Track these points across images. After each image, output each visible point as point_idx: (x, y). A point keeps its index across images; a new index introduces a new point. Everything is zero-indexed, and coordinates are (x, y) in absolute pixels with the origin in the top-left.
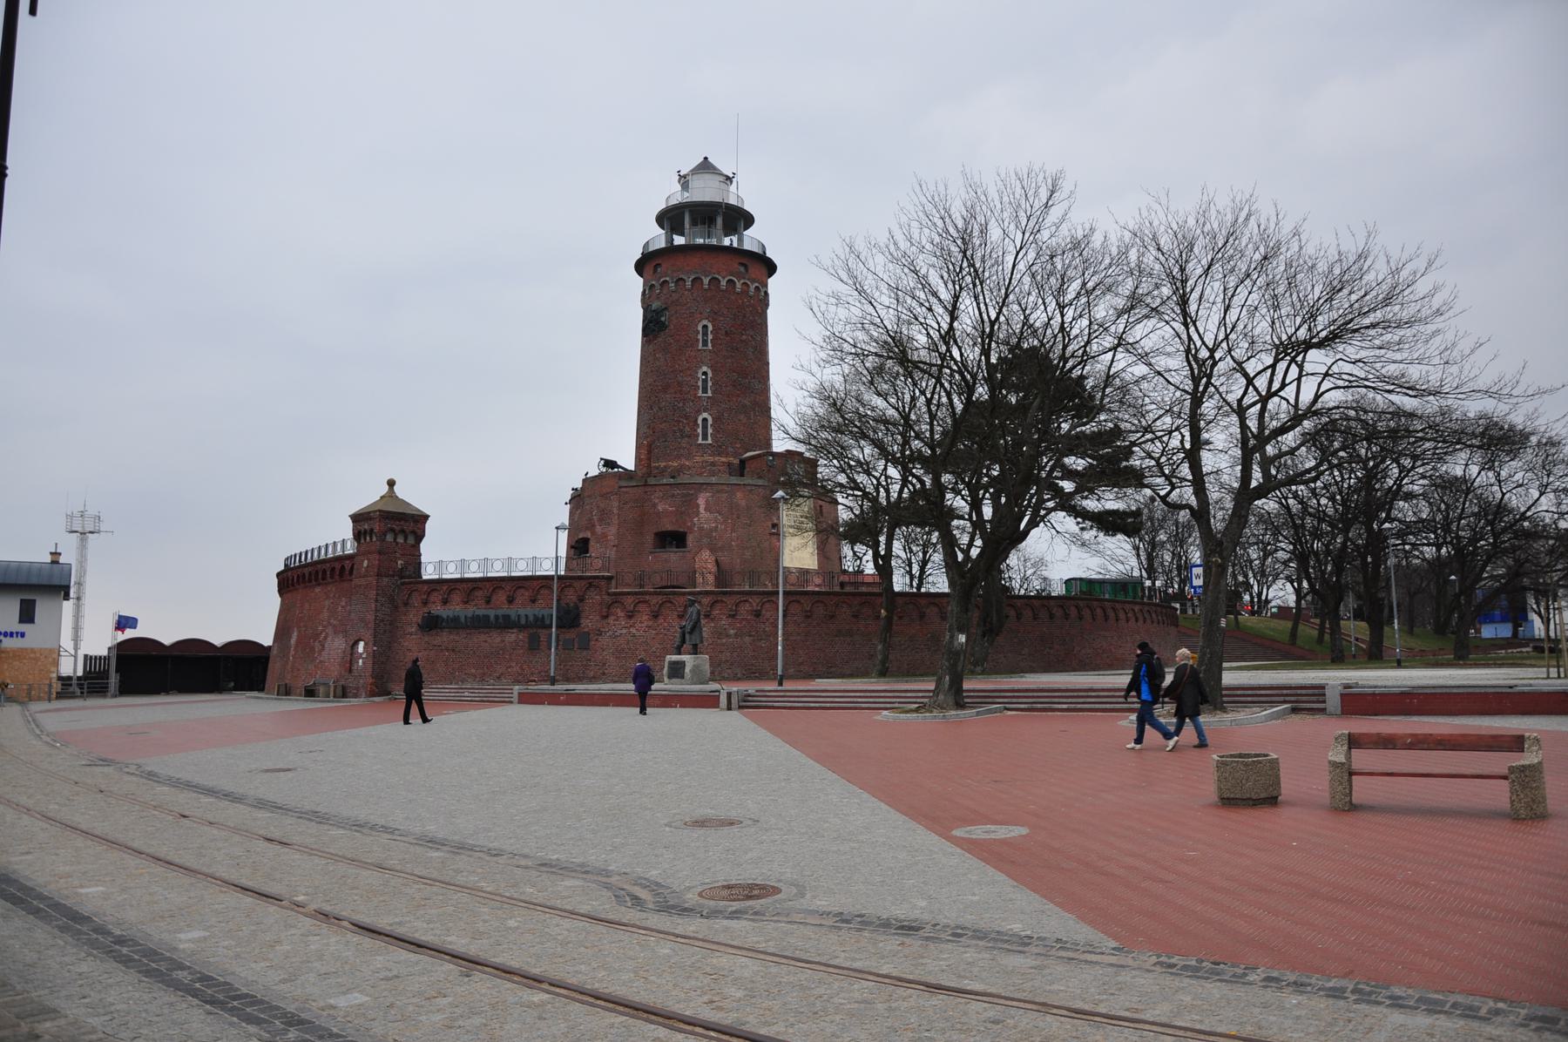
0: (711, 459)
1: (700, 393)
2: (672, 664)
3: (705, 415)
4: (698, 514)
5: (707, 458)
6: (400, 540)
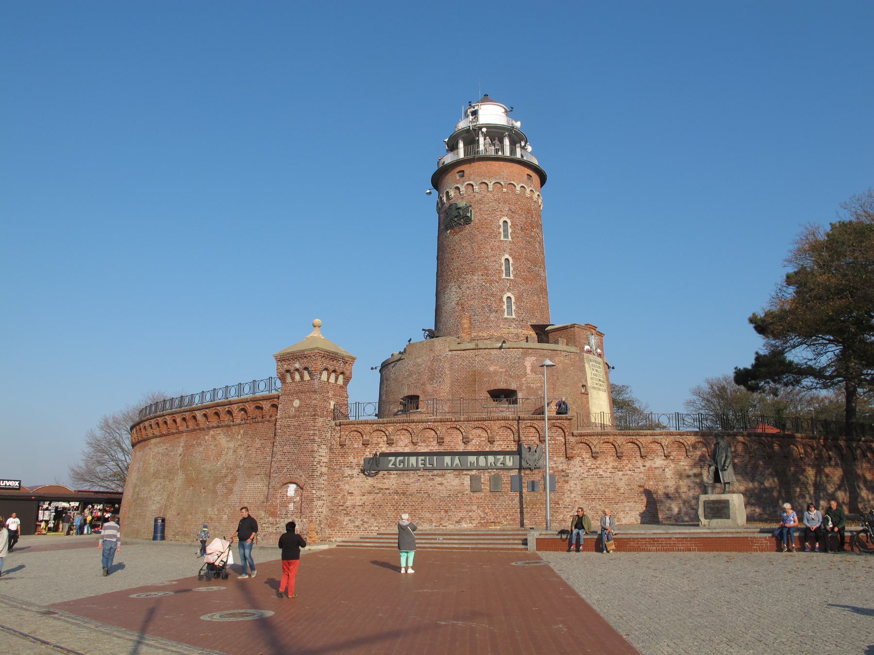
0: (515, 331)
1: (504, 276)
2: (725, 504)
3: (509, 294)
4: (525, 374)
6: (332, 379)
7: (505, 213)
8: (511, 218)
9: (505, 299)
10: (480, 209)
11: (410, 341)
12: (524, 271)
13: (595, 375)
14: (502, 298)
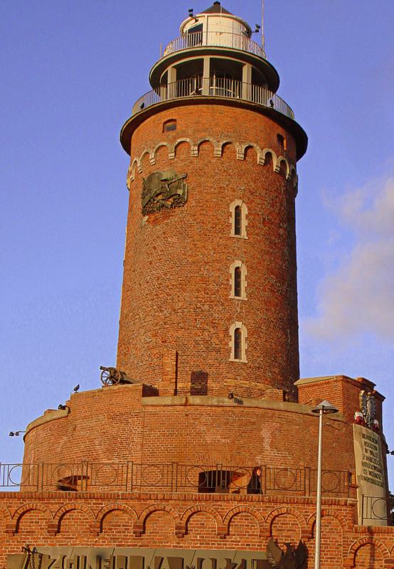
0: (246, 384)
3: (239, 325)
4: (261, 451)
5: (241, 382)
7: (240, 193)
8: (249, 203)
9: (232, 333)
10: (199, 185)
11: (77, 388)
12: (264, 290)
13: (370, 459)
14: (227, 330)
